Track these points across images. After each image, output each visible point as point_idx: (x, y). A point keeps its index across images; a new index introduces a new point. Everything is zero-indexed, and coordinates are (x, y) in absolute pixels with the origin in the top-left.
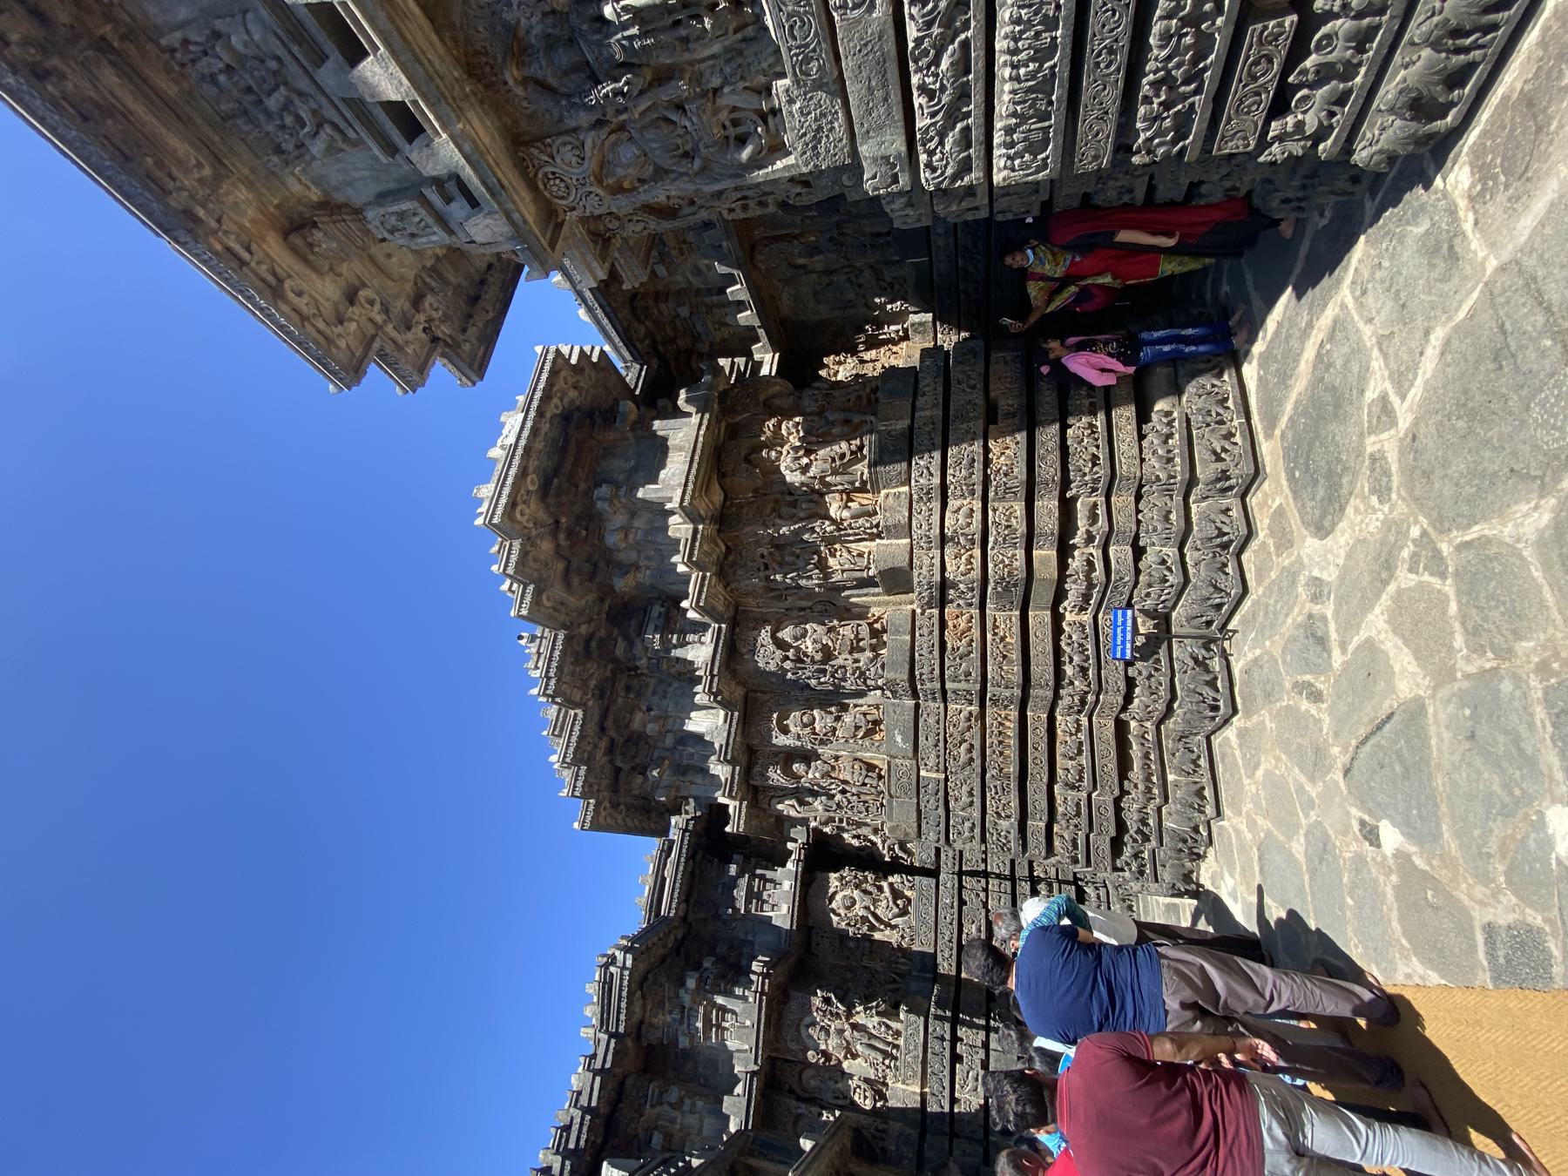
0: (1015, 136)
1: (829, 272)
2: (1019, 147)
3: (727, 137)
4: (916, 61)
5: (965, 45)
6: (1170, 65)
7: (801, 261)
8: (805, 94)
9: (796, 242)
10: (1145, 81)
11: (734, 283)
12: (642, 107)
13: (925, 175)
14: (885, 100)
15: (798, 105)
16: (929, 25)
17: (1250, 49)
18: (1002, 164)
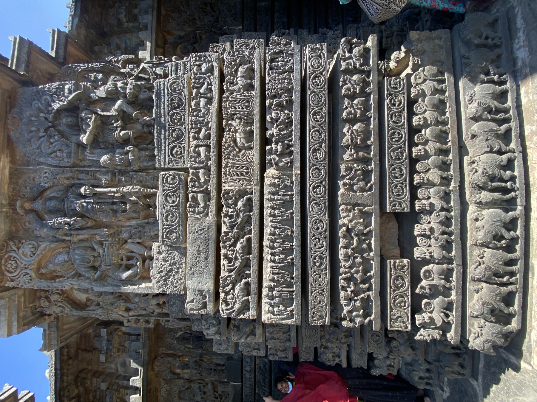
0: (274, 293)
1: (190, 381)
2: (277, 300)
3: (121, 265)
4: (224, 242)
5: (249, 240)
6: (352, 271)
7: (178, 371)
8: (168, 251)
9: (178, 359)
10: (340, 277)
11: (137, 375)
12: (81, 237)
13: (222, 306)
14: (206, 259)
15: (163, 255)
16: (232, 227)
17: (391, 271)
18: (267, 309)
